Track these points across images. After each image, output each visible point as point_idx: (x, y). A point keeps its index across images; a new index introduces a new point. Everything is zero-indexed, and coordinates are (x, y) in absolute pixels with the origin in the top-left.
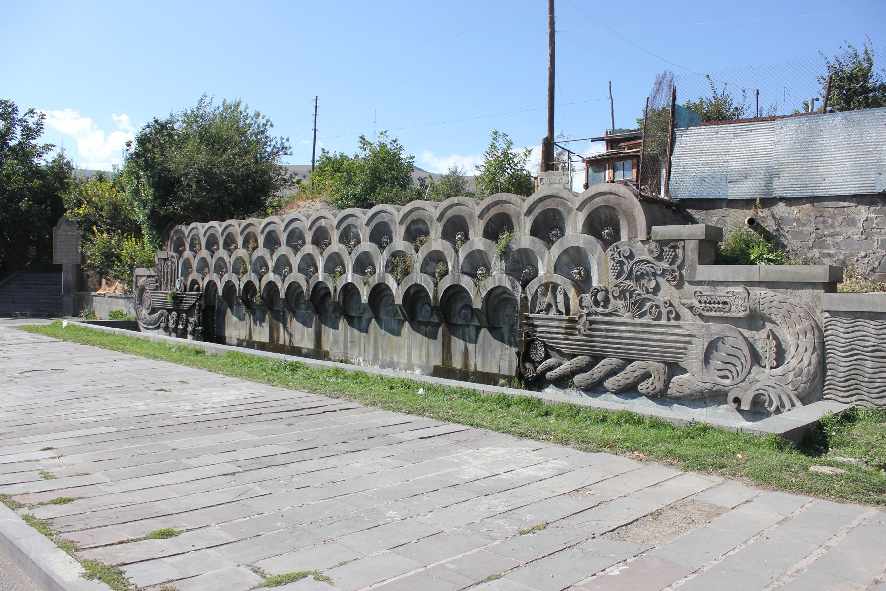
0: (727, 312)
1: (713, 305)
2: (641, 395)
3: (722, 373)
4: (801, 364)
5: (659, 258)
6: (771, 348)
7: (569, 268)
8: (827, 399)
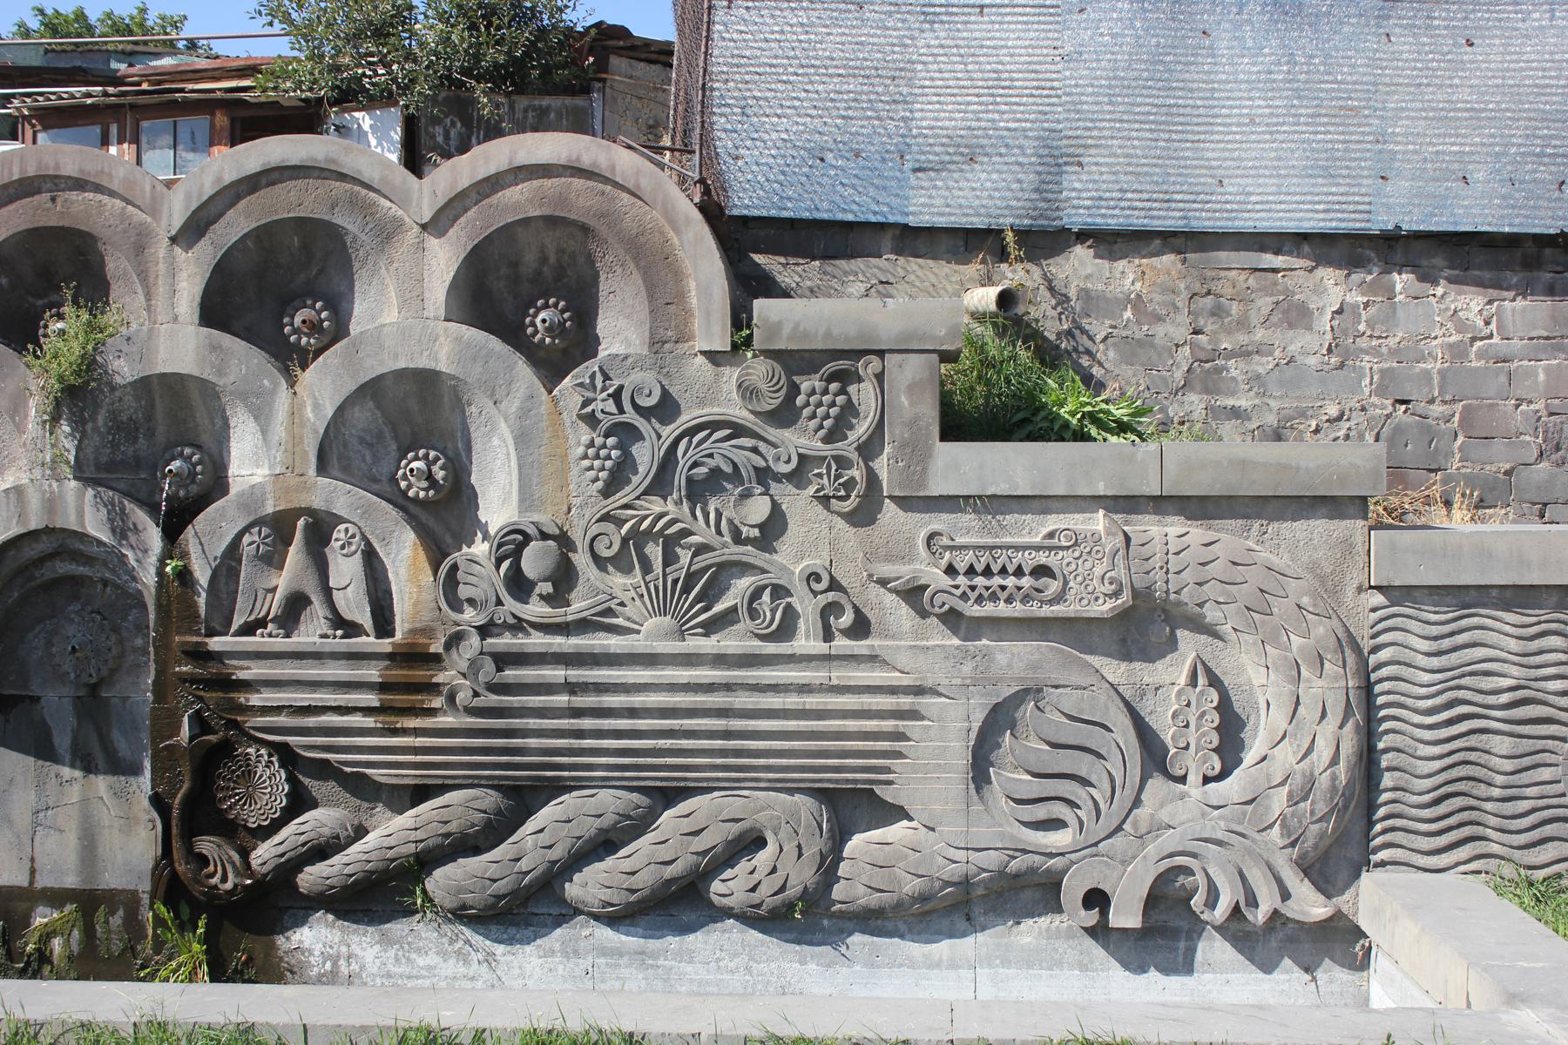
0: (1051, 602)
1: (997, 581)
3: (1041, 812)
4: (1307, 760)
5: (785, 415)
6: (1203, 714)
8: (1383, 864)
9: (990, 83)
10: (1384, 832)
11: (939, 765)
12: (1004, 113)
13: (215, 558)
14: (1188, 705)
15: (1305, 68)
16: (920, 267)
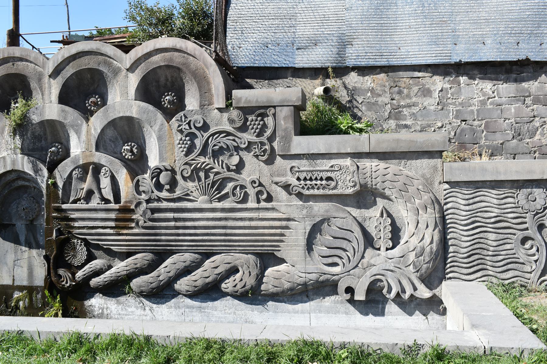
0: (332, 189)
1: (314, 182)
2: (225, 295)
3: (330, 260)
4: (422, 242)
5: (243, 128)
6: (385, 227)
7: (115, 145)
8: (450, 278)
9: (322, 19)
10: (450, 267)
11: (296, 245)
12: (326, 28)
13: (64, 179)
14: (380, 224)
15: (428, 8)
16: (301, 81)
